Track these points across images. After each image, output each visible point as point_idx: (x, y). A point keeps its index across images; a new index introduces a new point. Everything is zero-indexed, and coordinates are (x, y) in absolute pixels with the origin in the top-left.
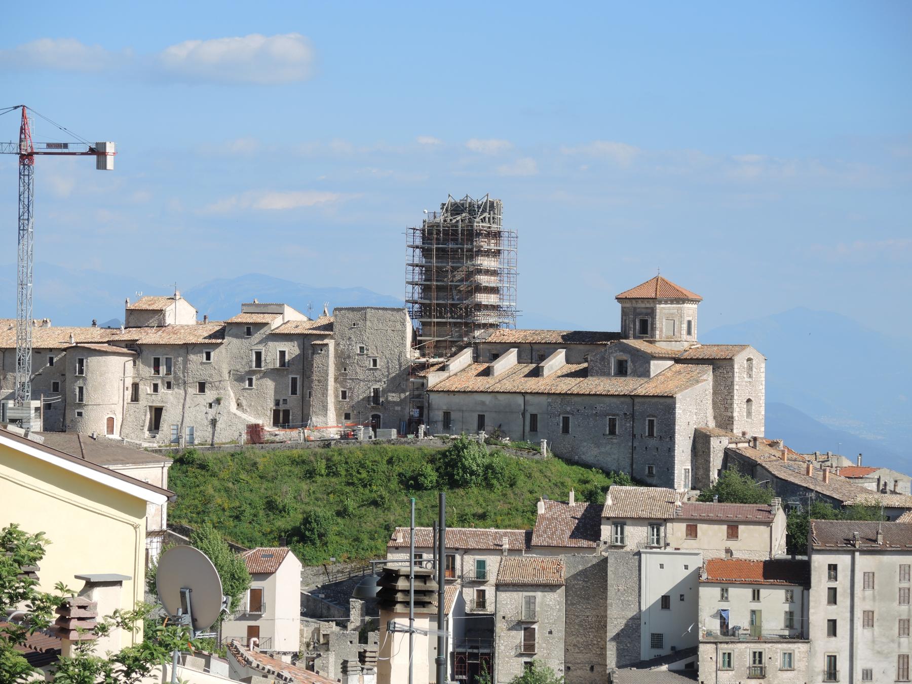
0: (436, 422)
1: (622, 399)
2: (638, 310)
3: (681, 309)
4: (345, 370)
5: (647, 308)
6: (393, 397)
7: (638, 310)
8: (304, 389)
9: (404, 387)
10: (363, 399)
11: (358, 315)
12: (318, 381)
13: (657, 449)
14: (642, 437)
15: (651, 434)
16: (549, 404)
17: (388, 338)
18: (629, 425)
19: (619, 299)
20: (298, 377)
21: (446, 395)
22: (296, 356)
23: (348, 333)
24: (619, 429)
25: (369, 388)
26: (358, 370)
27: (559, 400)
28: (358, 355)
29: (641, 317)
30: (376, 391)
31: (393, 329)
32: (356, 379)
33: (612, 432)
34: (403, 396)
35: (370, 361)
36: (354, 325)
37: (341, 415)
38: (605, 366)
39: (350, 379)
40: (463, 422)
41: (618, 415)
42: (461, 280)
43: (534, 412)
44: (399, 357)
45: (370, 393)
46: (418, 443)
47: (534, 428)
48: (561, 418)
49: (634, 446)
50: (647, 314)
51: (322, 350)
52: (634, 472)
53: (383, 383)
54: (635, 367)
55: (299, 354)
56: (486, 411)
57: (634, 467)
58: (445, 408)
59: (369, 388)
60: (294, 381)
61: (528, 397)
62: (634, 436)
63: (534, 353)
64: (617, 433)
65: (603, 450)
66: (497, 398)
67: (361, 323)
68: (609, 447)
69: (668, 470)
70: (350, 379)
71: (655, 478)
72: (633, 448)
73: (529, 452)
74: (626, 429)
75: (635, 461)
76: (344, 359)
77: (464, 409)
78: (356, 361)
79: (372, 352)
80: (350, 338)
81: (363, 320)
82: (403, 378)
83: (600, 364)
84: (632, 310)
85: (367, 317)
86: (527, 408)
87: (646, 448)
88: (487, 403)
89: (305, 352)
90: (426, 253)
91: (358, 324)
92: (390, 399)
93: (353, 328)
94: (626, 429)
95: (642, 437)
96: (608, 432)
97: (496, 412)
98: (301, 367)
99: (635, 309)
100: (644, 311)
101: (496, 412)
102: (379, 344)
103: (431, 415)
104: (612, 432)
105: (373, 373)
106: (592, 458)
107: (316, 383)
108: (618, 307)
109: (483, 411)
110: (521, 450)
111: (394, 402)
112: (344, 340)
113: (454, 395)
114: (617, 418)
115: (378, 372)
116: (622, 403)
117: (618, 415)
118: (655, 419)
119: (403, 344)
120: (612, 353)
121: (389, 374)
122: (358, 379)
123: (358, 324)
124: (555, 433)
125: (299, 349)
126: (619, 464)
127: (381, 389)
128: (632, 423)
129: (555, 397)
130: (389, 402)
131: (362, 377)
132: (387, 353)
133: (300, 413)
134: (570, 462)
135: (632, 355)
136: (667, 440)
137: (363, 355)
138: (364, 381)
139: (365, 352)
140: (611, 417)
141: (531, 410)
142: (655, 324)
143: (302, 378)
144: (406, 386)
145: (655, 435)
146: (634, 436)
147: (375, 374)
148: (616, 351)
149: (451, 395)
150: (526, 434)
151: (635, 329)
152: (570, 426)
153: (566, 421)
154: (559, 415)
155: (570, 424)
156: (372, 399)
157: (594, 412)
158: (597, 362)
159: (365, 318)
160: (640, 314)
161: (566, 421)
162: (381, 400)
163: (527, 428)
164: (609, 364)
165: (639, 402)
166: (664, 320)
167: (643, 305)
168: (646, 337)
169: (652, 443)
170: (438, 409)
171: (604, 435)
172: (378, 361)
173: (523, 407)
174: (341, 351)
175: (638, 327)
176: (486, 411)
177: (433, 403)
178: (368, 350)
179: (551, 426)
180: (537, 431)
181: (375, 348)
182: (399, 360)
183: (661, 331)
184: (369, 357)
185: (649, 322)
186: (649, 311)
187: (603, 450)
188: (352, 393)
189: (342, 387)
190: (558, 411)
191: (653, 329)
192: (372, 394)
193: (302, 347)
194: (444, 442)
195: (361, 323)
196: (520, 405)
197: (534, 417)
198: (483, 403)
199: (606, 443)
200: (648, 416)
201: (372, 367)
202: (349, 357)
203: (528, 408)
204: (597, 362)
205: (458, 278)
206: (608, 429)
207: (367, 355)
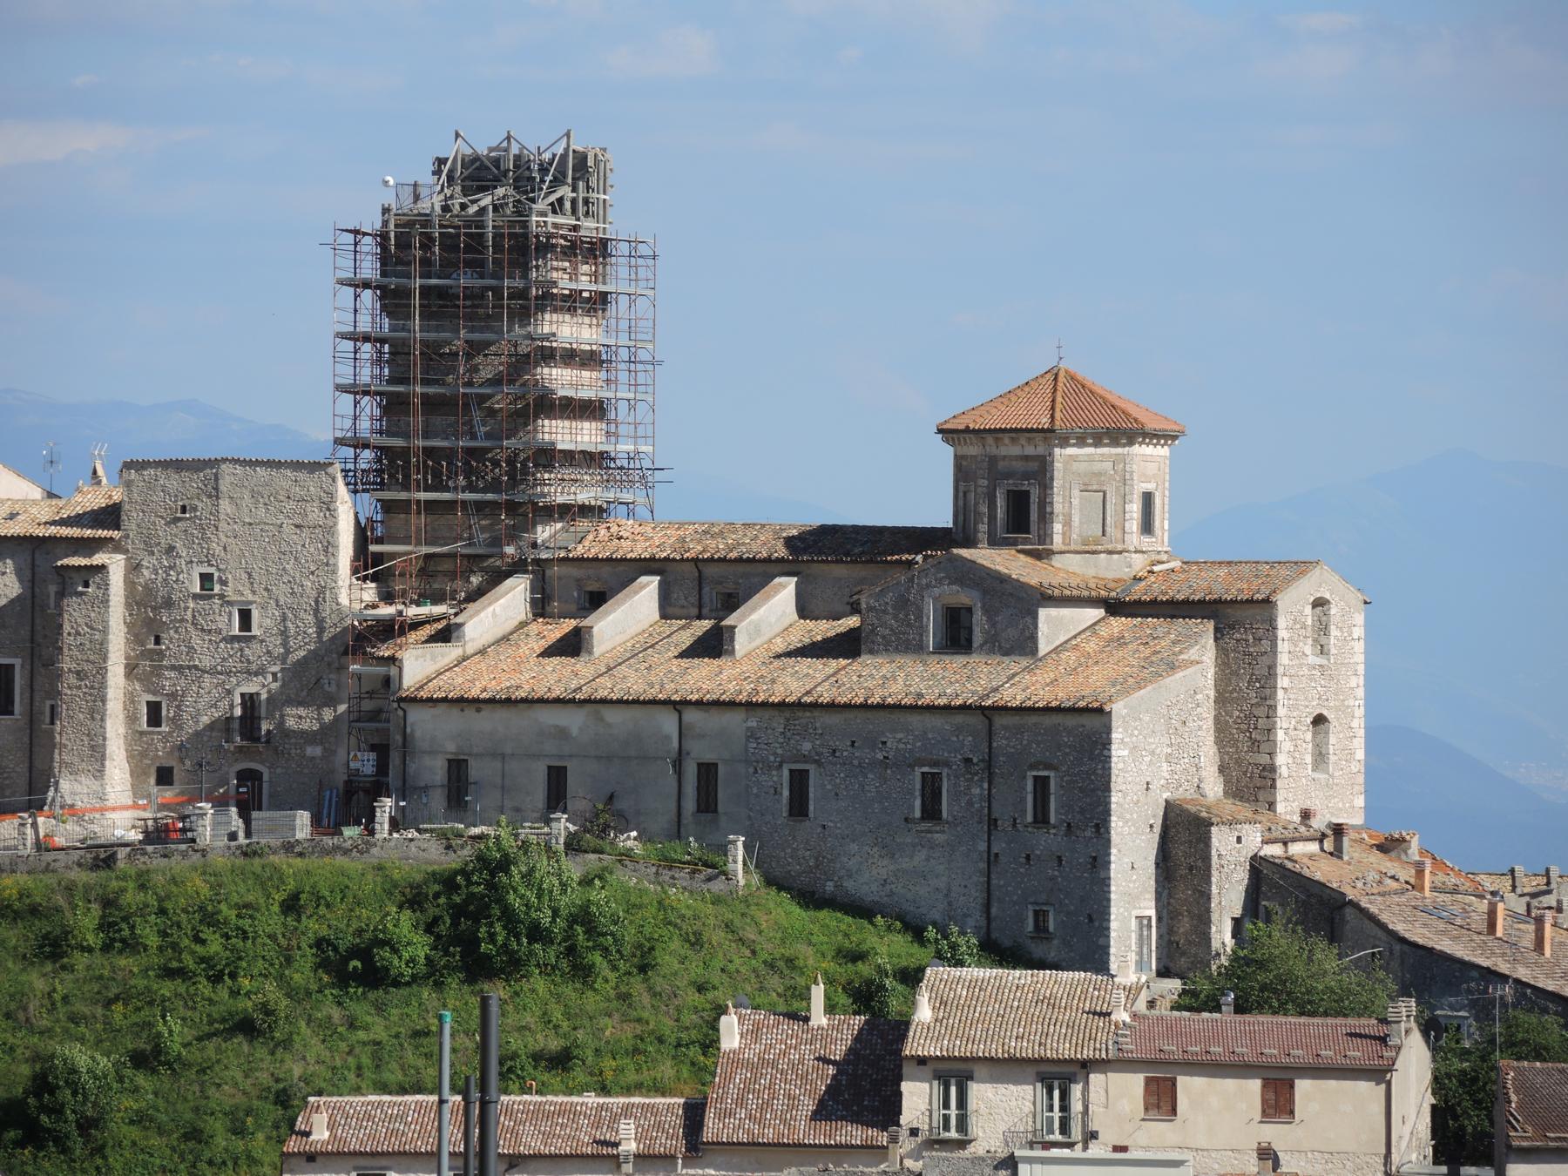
0: (426, 789)
1: (959, 719)
2: (1001, 465)
3: (1123, 459)
4: (158, 641)
5: (1027, 458)
6: (300, 719)
7: (1001, 465)
8: (37, 698)
9: (333, 689)
10: (211, 727)
11: (194, 482)
12: (78, 673)
13: (1060, 859)
15: (1041, 818)
16: (751, 735)
17: (284, 547)
18: (978, 791)
19: (946, 433)
20: (17, 662)
21: (455, 711)
22: (12, 601)
23: (165, 534)
25: (229, 692)
26: (196, 641)
27: (778, 722)
28: (195, 597)
29: (1010, 484)
30: (250, 701)
31: (299, 521)
32: (189, 667)
33: (931, 812)
34: (328, 715)
36: (184, 509)
37: (145, 773)
38: (909, 625)
39: (173, 668)
40: (503, 787)
41: (947, 764)
42: (496, 381)
43: (709, 757)
44: (317, 602)
45: (232, 706)
46: (374, 851)
47: (707, 802)
48: (786, 773)
49: (995, 850)
50: (1027, 476)
51: (86, 585)
52: (993, 925)
53: (270, 678)
54: (994, 625)
55: (19, 597)
56: (570, 756)
57: (994, 911)
58: (451, 747)
59: (229, 692)
61: (691, 716)
62: (993, 823)
63: (706, 590)
64: (945, 815)
66: (602, 720)
67: (203, 505)
68: (920, 856)
69: (1091, 919)
70: (173, 668)
71: (1055, 942)
72: (992, 859)
73: (694, 872)
74: (970, 803)
75: (996, 894)
76: (154, 609)
77: (508, 751)
78: (189, 616)
79: (237, 589)
80: (171, 549)
81: (210, 496)
82: (329, 664)
83: (895, 617)
85: (223, 488)
86: (687, 745)
87: (1028, 857)
88: (575, 731)
89: (37, 590)
90: (392, 300)
92: (291, 723)
93: (180, 519)
94: (970, 803)
96: (918, 814)
97: (599, 758)
98: (25, 632)
99: (993, 460)
100: (1019, 466)
101: (599, 758)
102: (257, 567)
103: (412, 768)
104: (931, 812)
105: (241, 650)
106: (874, 888)
107: (72, 680)
108: (945, 455)
109: (561, 757)
110: (670, 868)
111: (303, 732)
112: (153, 553)
113: (478, 710)
114: (945, 771)
115: (255, 645)
117: (947, 764)
118: (1052, 774)
119: (327, 564)
120: (928, 586)
121: (288, 652)
122: (196, 667)
123: (195, 509)
125: (21, 581)
126: (950, 904)
127: (264, 696)
128: (986, 785)
129: (767, 714)
130: (287, 733)
131: (206, 662)
132: (281, 591)
133: (23, 768)
134: (811, 899)
135: (985, 592)
136: (1088, 834)
137: (210, 597)
138: (213, 672)
139: (217, 588)
140: (926, 769)
141: (702, 751)
142: (1052, 503)
143: (28, 667)
144: (338, 686)
145: (1052, 820)
146: (993, 823)
147: (247, 652)
148: (940, 581)
149: (470, 712)
150: (684, 821)
152: (811, 795)
153: (799, 781)
154: (780, 766)
155: (811, 790)
156: (236, 725)
157: (880, 756)
158: (885, 612)
159: (216, 489)
160: (1009, 475)
161: (799, 781)
162: (265, 726)
163: (690, 805)
164: (919, 617)
165: (1005, 728)
166: (1076, 492)
167: (1015, 450)
168: (1026, 541)
170: (432, 753)
171: (906, 820)
172: (255, 614)
173: (675, 744)
174: (146, 587)
175: (1000, 513)
177: (418, 734)
178: (224, 583)
179: (757, 796)
180: (715, 811)
181: (245, 576)
182: (316, 611)
183: (1068, 523)
184: (230, 603)
185: (1034, 499)
186: (1034, 466)
188: (178, 707)
189: (148, 691)
190: (775, 754)
191: (1046, 517)
192: (238, 712)
193: (28, 573)
194: (448, 847)
195: (203, 505)
196: (668, 738)
197: (707, 772)
198: (562, 733)
199: (914, 846)
200: (1032, 767)
201: (236, 632)
202: (168, 603)
203: (689, 745)
204: (885, 612)
205: (486, 373)
206: (918, 803)
207: (222, 597)
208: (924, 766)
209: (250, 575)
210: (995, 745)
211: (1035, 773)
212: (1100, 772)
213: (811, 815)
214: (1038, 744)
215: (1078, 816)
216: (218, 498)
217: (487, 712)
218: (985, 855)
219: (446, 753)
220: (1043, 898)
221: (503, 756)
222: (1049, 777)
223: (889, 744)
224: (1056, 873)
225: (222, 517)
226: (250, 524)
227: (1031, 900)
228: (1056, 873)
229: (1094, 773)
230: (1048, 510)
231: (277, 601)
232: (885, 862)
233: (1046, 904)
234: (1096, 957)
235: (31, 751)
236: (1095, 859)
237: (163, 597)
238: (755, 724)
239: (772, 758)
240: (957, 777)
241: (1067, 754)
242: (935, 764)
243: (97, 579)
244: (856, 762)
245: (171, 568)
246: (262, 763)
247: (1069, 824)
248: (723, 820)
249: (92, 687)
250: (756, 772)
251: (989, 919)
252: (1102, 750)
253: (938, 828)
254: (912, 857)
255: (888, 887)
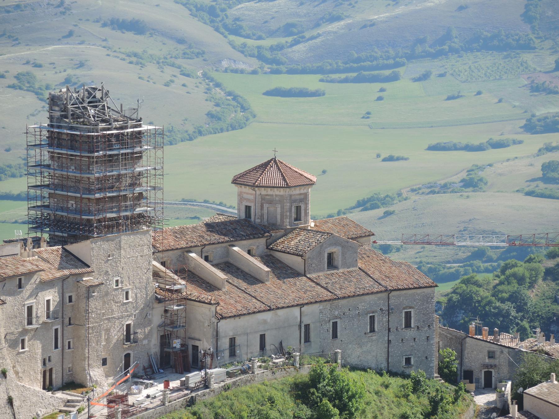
1: (379, 295)
5: (301, 194)
7: (293, 197)
8: (64, 340)
13: (415, 339)
14: (397, 329)
15: (408, 325)
24: (377, 326)
27: (328, 305)
33: (372, 330)
35: (123, 294)
44: (146, 284)
48: (331, 323)
49: (390, 339)
50: (301, 201)
56: (268, 330)
58: (231, 334)
60: (56, 330)
65: (365, 349)
69: (426, 358)
71: (413, 368)
72: (389, 342)
74: (383, 324)
75: (390, 354)
77: (249, 331)
81: (118, 249)
84: (289, 198)
87: (402, 340)
88: (269, 320)
91: (113, 255)
95: (397, 329)
97: (276, 329)
99: (291, 196)
104: (372, 330)
116: (379, 299)
117: (376, 312)
118: (412, 310)
123: (113, 255)
124: (326, 341)
128: (387, 317)
129: (325, 303)
133: (60, 369)
135: (342, 247)
141: (306, 321)
144: (152, 315)
146: (389, 330)
151: (291, 216)
153: (335, 325)
154: (329, 321)
159: (120, 246)
160: (295, 201)
161: (335, 325)
168: (301, 224)
169: (409, 333)
173: (299, 319)
176: (268, 330)
178: (122, 282)
179: (323, 333)
186: (302, 197)
187: (365, 349)
188: (108, 334)
190: (328, 317)
196: (296, 317)
198: (265, 322)
200: (404, 309)
208: (370, 313)
209: (129, 277)
210: (390, 302)
211: (406, 311)
212: (430, 307)
213: (339, 337)
214: (406, 300)
215: (422, 323)
216: (120, 249)
217: (242, 318)
218: (387, 341)
219: (229, 336)
220: (409, 353)
221: (247, 334)
222: (410, 311)
223: (360, 308)
224: (414, 344)
225: (122, 256)
226: (129, 258)
227: (404, 354)
228: (414, 344)
229: (428, 308)
230: (308, 212)
231: (136, 286)
232: (359, 350)
233: (410, 355)
234: (429, 370)
235: (63, 362)
236: (428, 337)
237: (105, 292)
238: (322, 308)
239: (327, 319)
240: (379, 316)
241: (418, 302)
242: (373, 312)
243: (98, 289)
244: (351, 316)
245: (107, 280)
246: (131, 350)
247: (418, 327)
248: (313, 344)
249: (97, 332)
250: (322, 325)
251: (388, 364)
252: (431, 300)
253: (374, 335)
254: (366, 346)
255: (360, 358)
